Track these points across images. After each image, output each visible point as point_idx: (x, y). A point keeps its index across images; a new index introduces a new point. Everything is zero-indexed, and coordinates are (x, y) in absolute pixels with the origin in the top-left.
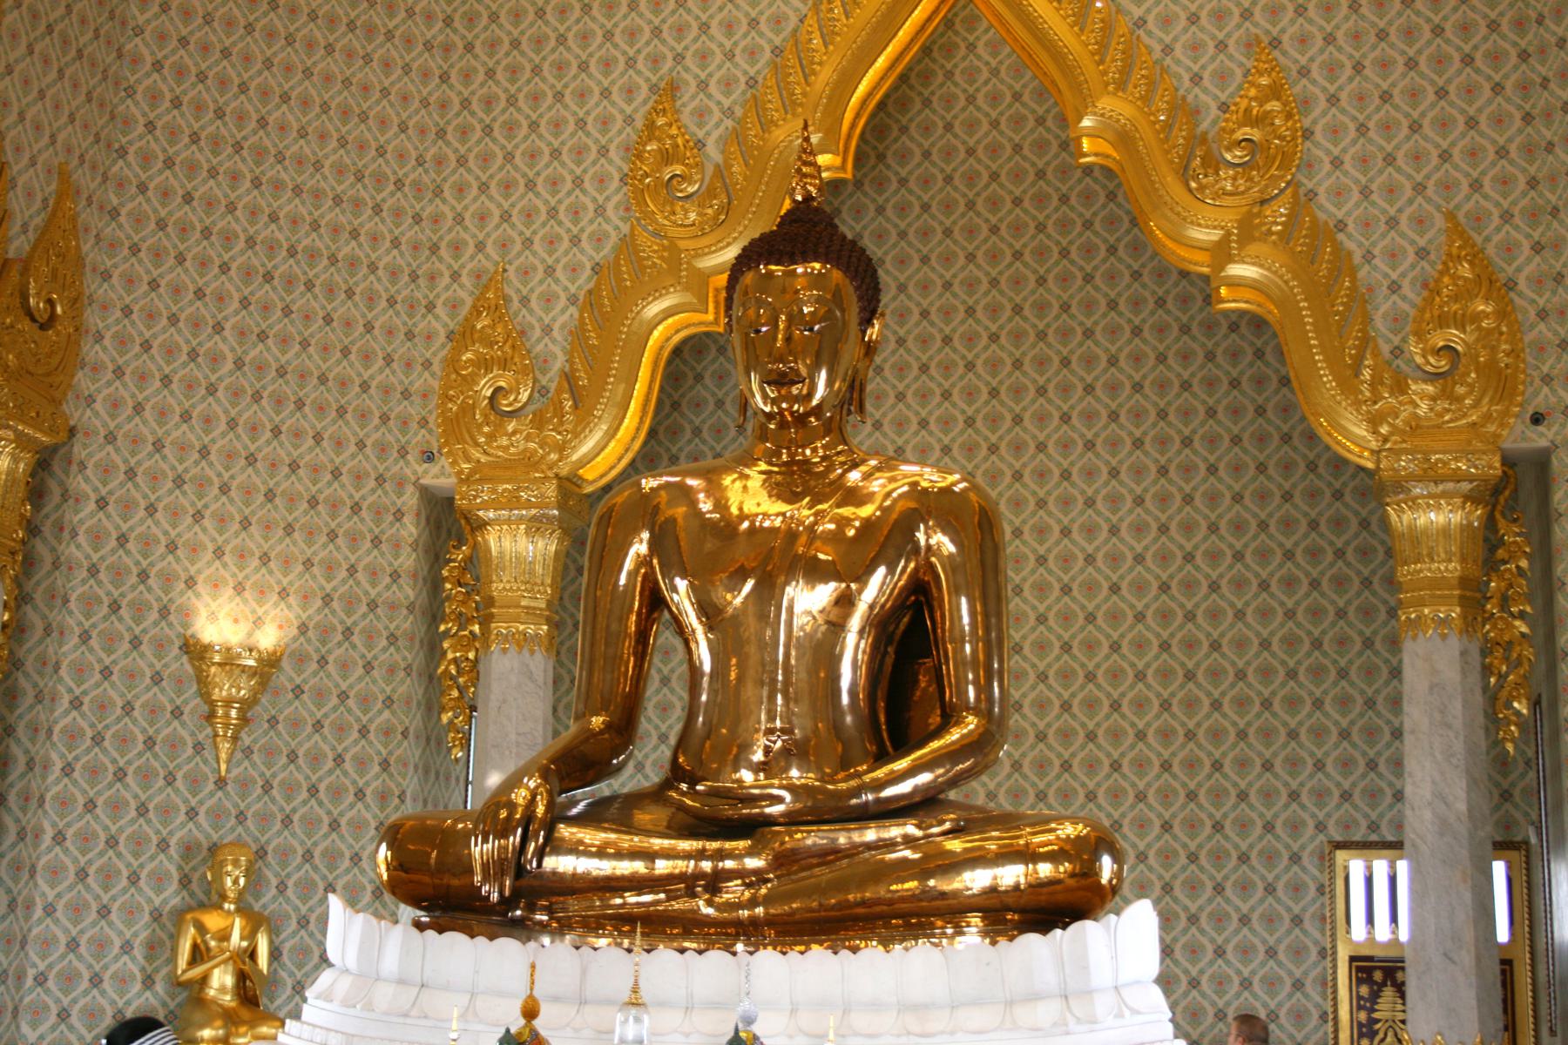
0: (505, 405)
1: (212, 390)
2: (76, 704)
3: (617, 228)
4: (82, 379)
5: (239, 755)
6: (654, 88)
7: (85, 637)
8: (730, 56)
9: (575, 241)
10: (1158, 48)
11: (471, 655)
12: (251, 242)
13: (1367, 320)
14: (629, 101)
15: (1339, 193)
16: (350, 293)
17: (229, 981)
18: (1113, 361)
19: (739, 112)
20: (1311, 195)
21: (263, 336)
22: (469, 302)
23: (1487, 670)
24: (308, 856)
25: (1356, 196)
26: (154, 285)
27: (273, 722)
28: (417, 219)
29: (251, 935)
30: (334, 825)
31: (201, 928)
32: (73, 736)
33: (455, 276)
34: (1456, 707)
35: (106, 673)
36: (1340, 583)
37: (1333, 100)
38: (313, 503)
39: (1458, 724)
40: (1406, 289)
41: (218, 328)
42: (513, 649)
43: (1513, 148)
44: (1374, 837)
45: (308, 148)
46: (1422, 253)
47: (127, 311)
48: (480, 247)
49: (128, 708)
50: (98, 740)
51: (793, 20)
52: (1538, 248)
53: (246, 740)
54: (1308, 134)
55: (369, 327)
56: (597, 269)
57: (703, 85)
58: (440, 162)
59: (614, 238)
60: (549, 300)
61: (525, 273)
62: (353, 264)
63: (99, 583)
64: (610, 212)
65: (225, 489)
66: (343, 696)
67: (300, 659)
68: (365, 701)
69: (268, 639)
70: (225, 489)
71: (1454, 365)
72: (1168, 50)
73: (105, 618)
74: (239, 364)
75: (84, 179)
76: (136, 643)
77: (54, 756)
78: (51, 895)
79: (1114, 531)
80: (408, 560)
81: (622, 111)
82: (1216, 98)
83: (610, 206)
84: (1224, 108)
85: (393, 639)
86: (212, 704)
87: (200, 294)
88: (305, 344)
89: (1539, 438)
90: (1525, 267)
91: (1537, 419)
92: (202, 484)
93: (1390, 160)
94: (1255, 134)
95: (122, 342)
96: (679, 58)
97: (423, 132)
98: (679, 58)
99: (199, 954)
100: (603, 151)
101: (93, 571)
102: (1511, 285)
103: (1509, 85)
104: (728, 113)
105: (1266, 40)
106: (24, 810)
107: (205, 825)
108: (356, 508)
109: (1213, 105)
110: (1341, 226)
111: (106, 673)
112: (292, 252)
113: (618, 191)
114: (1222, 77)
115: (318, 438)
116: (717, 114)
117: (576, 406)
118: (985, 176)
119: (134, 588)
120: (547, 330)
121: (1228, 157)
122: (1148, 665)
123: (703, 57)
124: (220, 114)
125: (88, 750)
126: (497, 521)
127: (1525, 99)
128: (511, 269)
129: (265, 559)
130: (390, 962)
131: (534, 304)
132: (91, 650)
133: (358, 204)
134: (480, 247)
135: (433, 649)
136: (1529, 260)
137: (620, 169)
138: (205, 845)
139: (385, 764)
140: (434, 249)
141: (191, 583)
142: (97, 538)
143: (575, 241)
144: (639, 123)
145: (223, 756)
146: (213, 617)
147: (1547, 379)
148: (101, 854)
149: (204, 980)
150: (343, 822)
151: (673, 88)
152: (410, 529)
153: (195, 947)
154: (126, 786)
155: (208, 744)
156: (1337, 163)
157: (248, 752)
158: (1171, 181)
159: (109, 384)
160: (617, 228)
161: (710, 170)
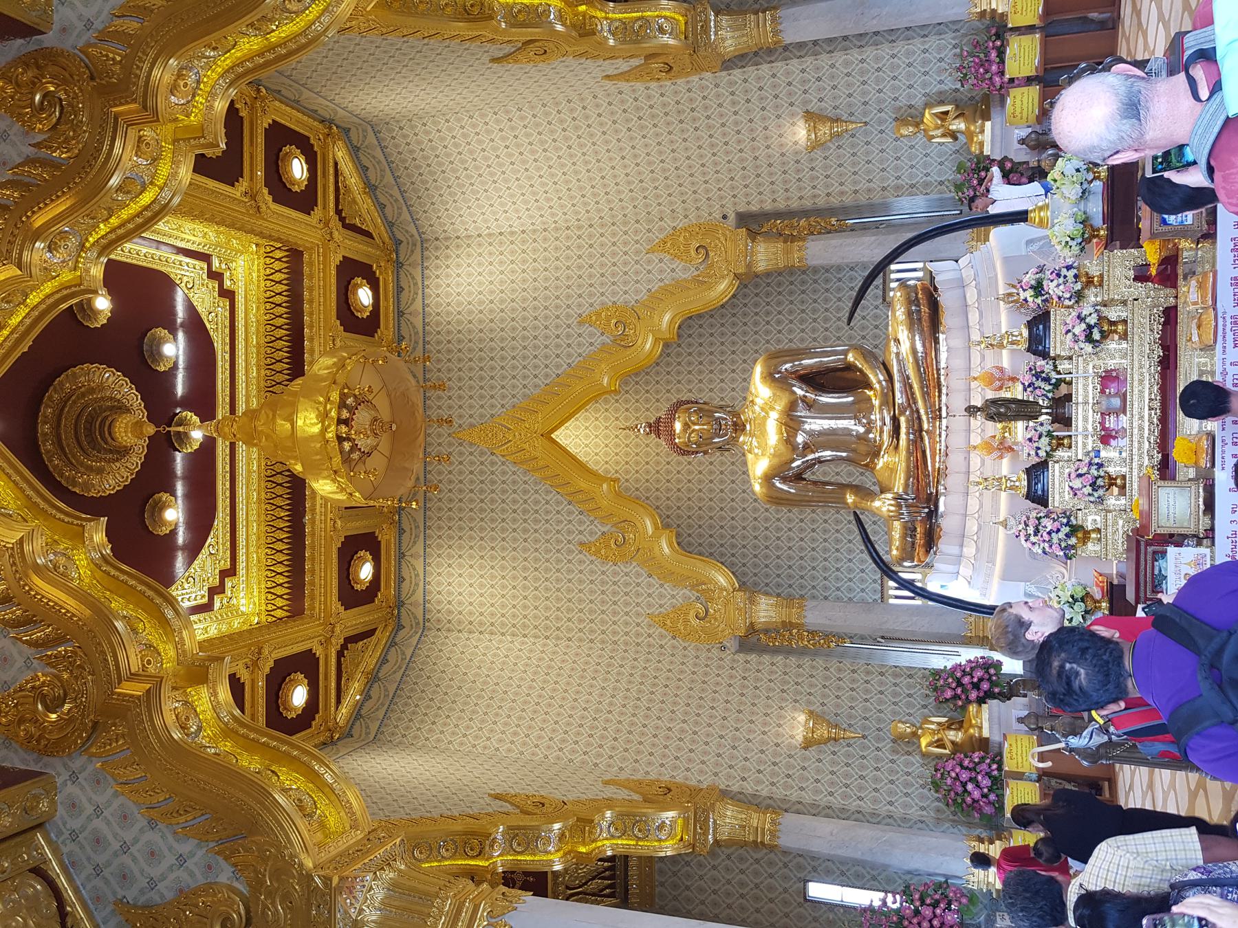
0: (702, 615)
1: (695, 733)
2: (831, 794)
4: (693, 783)
5: (852, 729)
6: (581, 552)
7: (802, 789)
8: (570, 522)
9: (638, 585)
11: (806, 634)
12: (634, 715)
13: (685, 280)
14: (585, 562)
15: (637, 292)
16: (656, 677)
17: (952, 733)
19: (592, 518)
20: (637, 301)
21: (673, 712)
22: (660, 630)
23: (820, 233)
24: (895, 704)
25: (638, 285)
26: (651, 754)
27: (836, 715)
28: (626, 651)
29: (933, 723)
30: (881, 693)
31: (929, 745)
32: (845, 796)
33: (649, 636)
34: (833, 242)
35: (817, 781)
36: (779, 303)
37: (602, 294)
38: (742, 695)
39: (840, 241)
40: (674, 266)
41: (670, 729)
42: (804, 613)
43: (624, 229)
44: (881, 287)
45: (596, 692)
46: (661, 261)
47: (662, 765)
48: (638, 625)
49: (833, 773)
50: (847, 786)
51: (559, 496)
52: (661, 219)
53: (845, 726)
54: (614, 303)
55: (669, 671)
56: (650, 576)
57: (581, 532)
58: (603, 642)
59: (638, 569)
60: (661, 596)
61: (650, 605)
62: (643, 676)
63: (778, 782)
64: (628, 570)
65: (737, 729)
66: (825, 687)
67: (809, 703)
68: (827, 678)
69: (802, 718)
70: (737, 729)
71: (704, 247)
72: (580, 355)
73: (793, 780)
74: (684, 721)
75: (608, 777)
76: (804, 768)
77: (854, 804)
78: (916, 808)
80: (766, 658)
83: (625, 570)
84: (602, 334)
85: (799, 666)
86: (829, 739)
87: (655, 736)
88: (676, 696)
89: (732, 216)
90: (668, 223)
91: (725, 217)
92: (735, 739)
93: (626, 273)
94: (614, 321)
95: (675, 768)
96: (569, 542)
97: (591, 648)
98: (569, 542)
99: (940, 744)
100: (603, 573)
101: (773, 784)
102: (674, 228)
103: (601, 231)
104: (592, 522)
105: (579, 319)
106: (879, 815)
107: (883, 744)
108: (744, 678)
110: (649, 290)
111: (817, 781)
112: (639, 699)
114: (591, 335)
115: (715, 692)
116: (592, 526)
117: (705, 584)
119: (780, 768)
120: (673, 597)
123: (569, 532)
124: (581, 726)
125: (851, 790)
126: (751, 617)
127: (606, 225)
128: (649, 612)
129: (766, 715)
130: (954, 550)
131: (663, 602)
132: (807, 787)
133: (619, 674)
134: (638, 625)
135: (803, 652)
138: (892, 744)
139: (854, 671)
140: (638, 644)
141: (777, 745)
142: (759, 782)
143: (638, 585)
144: (594, 558)
145: (852, 735)
146: (792, 737)
147: (710, 214)
148: (898, 787)
149: (953, 742)
150: (879, 689)
151: (581, 544)
152: (753, 657)
153: (937, 747)
154: (867, 775)
155: (847, 741)
156: (626, 293)
157: (850, 725)
158: (629, 351)
159: (693, 774)
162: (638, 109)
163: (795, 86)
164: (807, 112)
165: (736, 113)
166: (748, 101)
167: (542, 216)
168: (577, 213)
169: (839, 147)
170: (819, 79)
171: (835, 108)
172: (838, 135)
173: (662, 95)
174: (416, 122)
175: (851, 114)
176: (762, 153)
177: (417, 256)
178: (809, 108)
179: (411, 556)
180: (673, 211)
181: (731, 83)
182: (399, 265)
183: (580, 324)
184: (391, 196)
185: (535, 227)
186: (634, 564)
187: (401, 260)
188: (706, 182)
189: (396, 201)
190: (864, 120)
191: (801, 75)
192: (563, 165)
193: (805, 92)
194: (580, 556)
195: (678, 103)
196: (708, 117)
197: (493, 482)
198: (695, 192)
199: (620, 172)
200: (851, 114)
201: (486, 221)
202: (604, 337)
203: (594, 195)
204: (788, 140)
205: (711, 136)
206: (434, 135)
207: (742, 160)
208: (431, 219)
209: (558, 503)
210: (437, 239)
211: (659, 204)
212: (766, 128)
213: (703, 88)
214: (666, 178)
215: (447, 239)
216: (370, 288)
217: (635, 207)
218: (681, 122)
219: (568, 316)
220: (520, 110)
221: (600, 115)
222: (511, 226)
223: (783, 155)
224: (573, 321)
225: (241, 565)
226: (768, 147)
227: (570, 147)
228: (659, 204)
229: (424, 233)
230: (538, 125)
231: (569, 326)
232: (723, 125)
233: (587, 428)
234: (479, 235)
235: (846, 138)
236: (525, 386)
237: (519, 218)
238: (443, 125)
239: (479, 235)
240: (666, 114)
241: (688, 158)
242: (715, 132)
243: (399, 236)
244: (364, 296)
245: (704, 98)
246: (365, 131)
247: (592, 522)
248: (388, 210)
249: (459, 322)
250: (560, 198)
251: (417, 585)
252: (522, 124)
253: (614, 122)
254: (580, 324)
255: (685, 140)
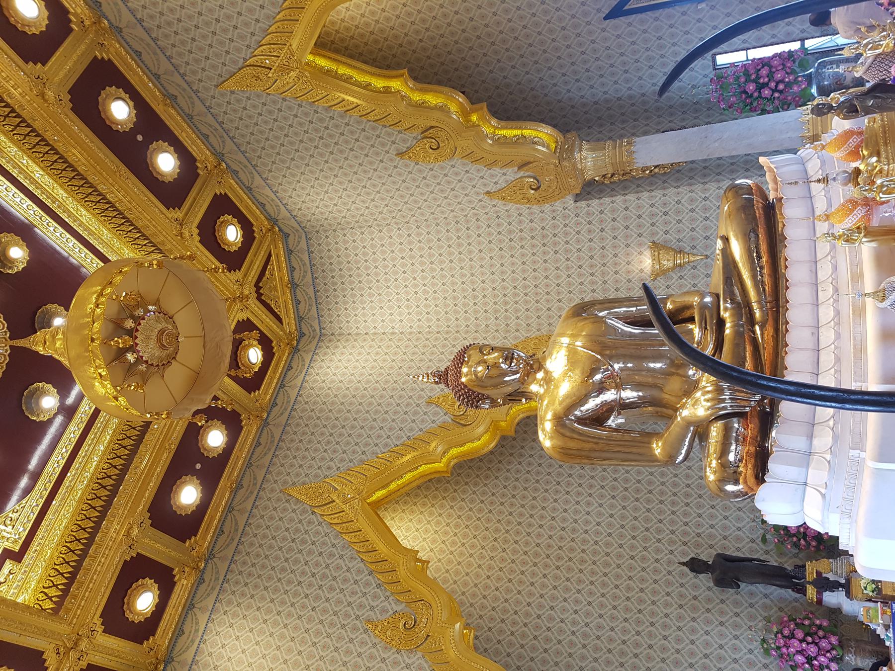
3: (418, 659)
10: (419, 433)
18: (523, 506)
19: (388, 594)
51: (362, 565)
52: (517, 331)
57: (372, 608)
59: (421, 661)
64: (410, 661)
72: (421, 430)
79: (588, 513)
81: (370, 648)
82: (442, 416)
84: (445, 414)
96: (357, 618)
98: (357, 618)
104: (387, 598)
109: (444, 417)
113: (402, 656)
116: (386, 603)
118: (442, 545)
121: (462, 413)
122: (644, 507)
123: (361, 606)
136: (521, 333)
137: (393, 653)
144: (377, 640)
151: (369, 621)
158: (465, 429)
160: (418, 659)
161: (408, 609)
162: (510, 232)
163: (644, 219)
164: (654, 242)
165: (591, 240)
166: (602, 230)
167: (419, 320)
168: (448, 320)
169: (681, 277)
170: (666, 214)
171: (679, 240)
172: (680, 266)
173: (531, 221)
174: (340, 233)
175: (694, 247)
176: (610, 278)
177: (312, 346)
178: (655, 239)
179: (200, 609)
180: (528, 325)
181: (589, 214)
182: (295, 350)
183: (429, 403)
184: (307, 294)
185: (413, 330)
186: (419, 654)
187: (299, 347)
188: (559, 301)
189: (310, 298)
190: (705, 253)
191: (651, 209)
192: (444, 277)
193: (653, 225)
194: (364, 636)
195: (543, 228)
196: (567, 242)
197: (304, 542)
198: (549, 309)
199: (488, 285)
200: (694, 247)
201: (374, 321)
202: (446, 417)
203: (465, 305)
204: (635, 267)
205: (568, 259)
206: (350, 245)
207: (592, 283)
208: (332, 316)
209: (359, 571)
210: (333, 334)
211: (518, 318)
212: (616, 255)
213: (565, 217)
214: (526, 295)
215: (340, 335)
216: (262, 350)
217: (497, 318)
218: (544, 245)
219: (420, 397)
220: (418, 227)
221: (479, 236)
222: (393, 328)
223: (629, 281)
224: (422, 402)
225: (27, 559)
226: (616, 273)
227: (451, 261)
228: (518, 318)
229: (324, 329)
230: (430, 241)
231: (418, 405)
232: (579, 250)
233: (417, 530)
234: (367, 334)
235: (687, 272)
236: (364, 453)
237: (401, 321)
238: (358, 237)
239: (367, 334)
240: (533, 238)
241: (547, 277)
242: (572, 256)
243: (305, 330)
244: (255, 355)
245: (566, 225)
246: (300, 237)
247: (387, 598)
248: (301, 307)
249: (327, 395)
250: (436, 306)
251: (193, 641)
252: (418, 240)
253: (490, 242)
254: (429, 403)
255: (545, 261)
